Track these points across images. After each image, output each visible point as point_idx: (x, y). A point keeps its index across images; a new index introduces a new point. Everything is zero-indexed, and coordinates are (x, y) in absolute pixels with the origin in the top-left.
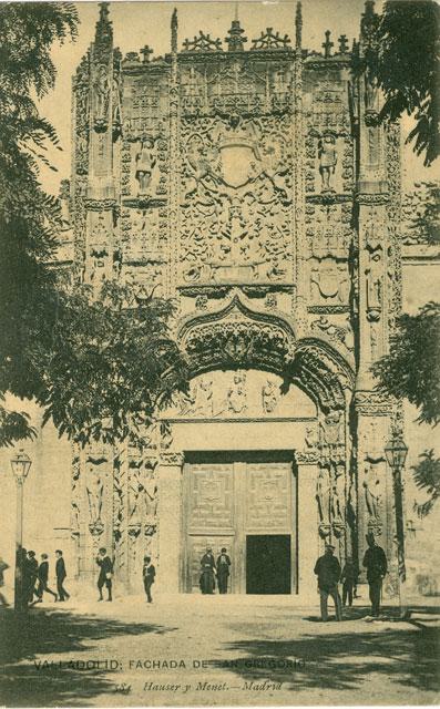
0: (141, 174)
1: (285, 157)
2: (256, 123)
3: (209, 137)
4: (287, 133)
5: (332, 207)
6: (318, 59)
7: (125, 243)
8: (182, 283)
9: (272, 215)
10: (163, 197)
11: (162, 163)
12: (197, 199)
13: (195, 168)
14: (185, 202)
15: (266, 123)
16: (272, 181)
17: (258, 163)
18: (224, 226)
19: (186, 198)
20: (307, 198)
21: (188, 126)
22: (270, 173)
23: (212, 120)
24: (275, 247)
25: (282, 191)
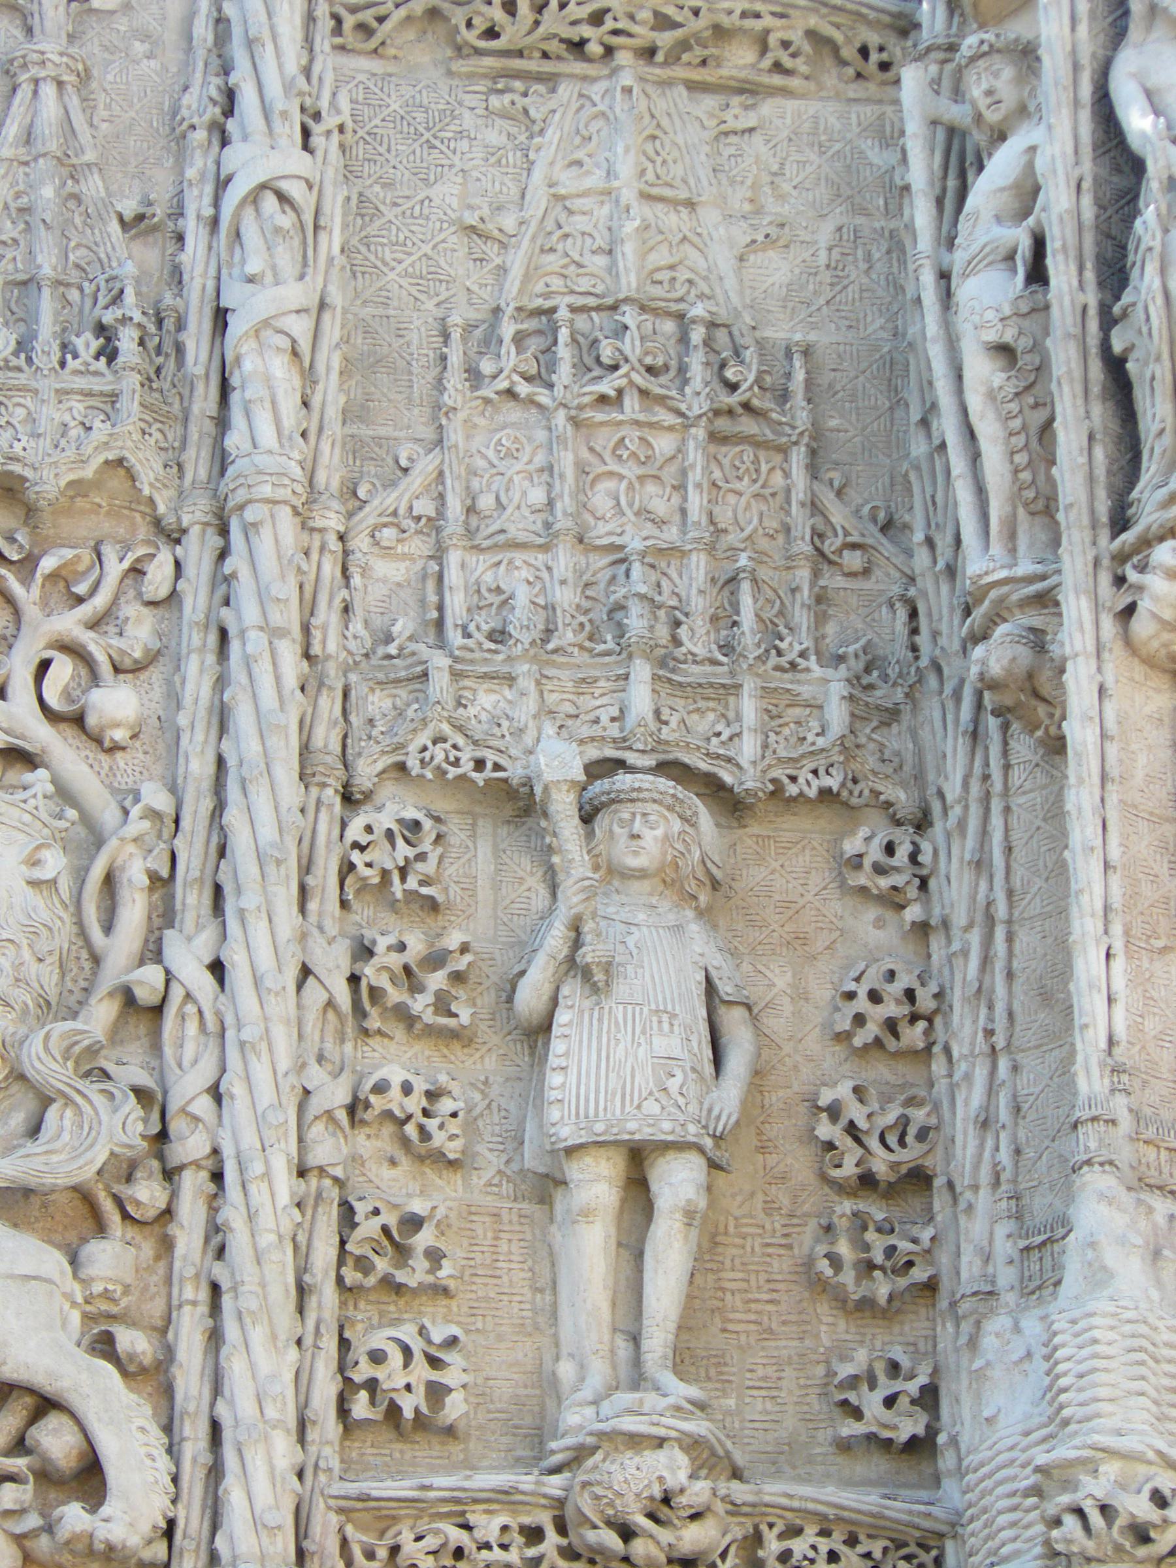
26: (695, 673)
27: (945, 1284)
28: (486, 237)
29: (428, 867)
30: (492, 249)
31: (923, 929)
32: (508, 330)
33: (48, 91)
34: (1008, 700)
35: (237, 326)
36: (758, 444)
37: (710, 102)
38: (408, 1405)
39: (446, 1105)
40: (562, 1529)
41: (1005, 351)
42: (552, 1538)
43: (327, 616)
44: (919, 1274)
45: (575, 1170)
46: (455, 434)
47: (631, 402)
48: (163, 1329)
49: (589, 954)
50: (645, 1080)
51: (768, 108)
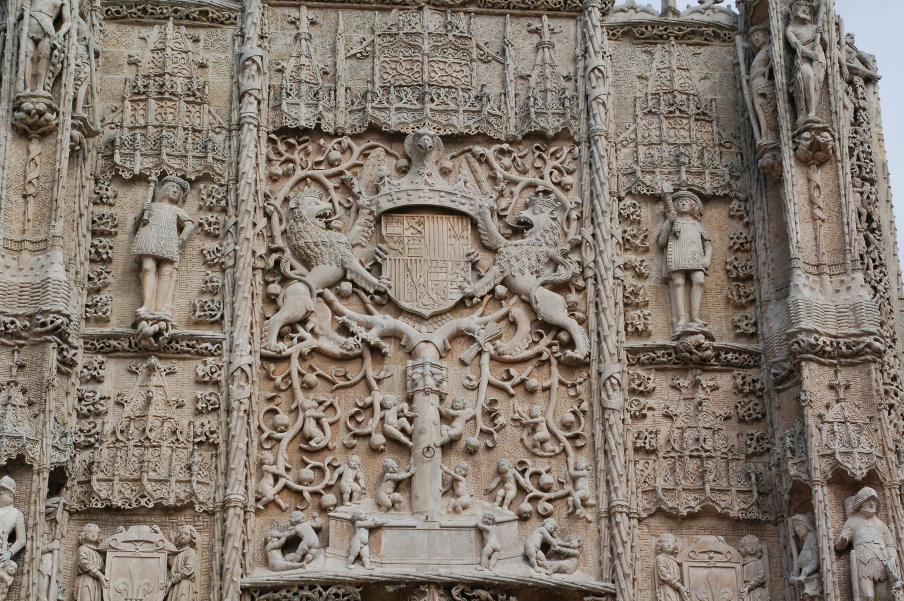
0: (149, 264)
1: (567, 247)
2: (482, 159)
3: (346, 187)
4: (565, 188)
5: (706, 380)
6: (646, 17)
7: (85, 455)
8: (260, 575)
9: (531, 392)
10: (208, 333)
11: (211, 245)
12: (311, 342)
13: (307, 263)
14: (275, 346)
15: (507, 161)
16: (528, 304)
17: (485, 259)
18: (391, 415)
19: (281, 337)
20: (631, 351)
21: (287, 155)
22: (526, 281)
23: (357, 149)
24: (547, 479)
25: (560, 328)
26: (694, 170)
27: (758, 299)
28: (643, 78)
29: (637, 213)
30: (644, 81)
31: (747, 225)
32: (650, 97)
33: (546, 49)
34: (767, 171)
35: (591, 98)
36: (707, 121)
37: (691, 48)
38: (640, 328)
39: (645, 264)
40: (676, 353)
41: (763, 95)
42: (674, 355)
43: (613, 160)
44: (751, 297)
45: (674, 276)
46: (638, 120)
47: (677, 113)
48: (585, 312)
49: (676, 228)
50: (690, 256)
51: (703, 49)
